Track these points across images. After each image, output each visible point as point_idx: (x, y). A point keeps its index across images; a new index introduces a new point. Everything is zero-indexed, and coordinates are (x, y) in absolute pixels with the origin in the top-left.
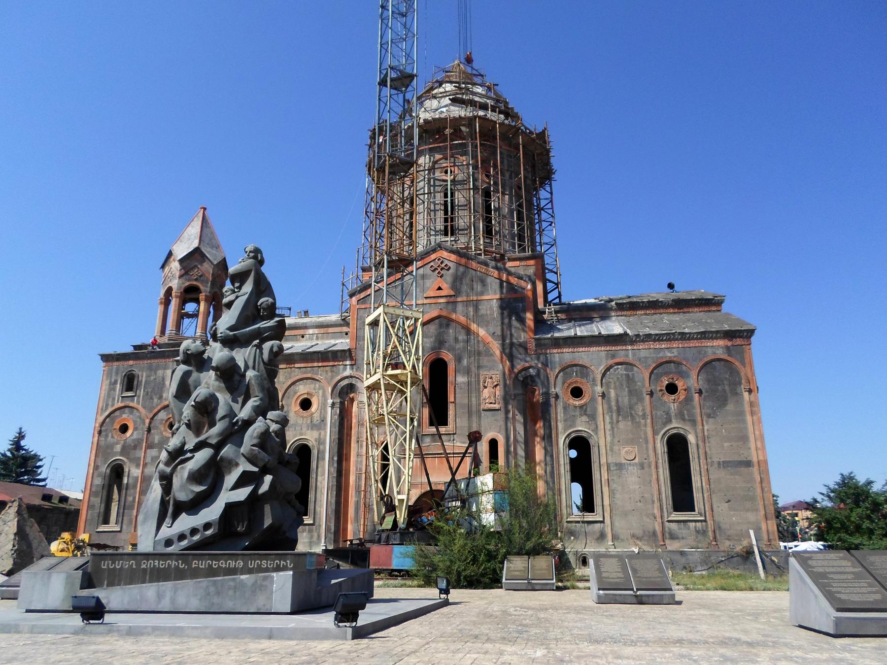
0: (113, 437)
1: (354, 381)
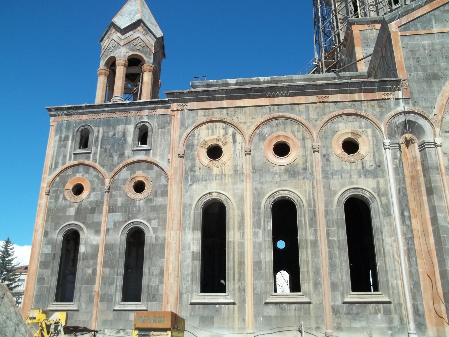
0: (64, 198)
1: (412, 117)
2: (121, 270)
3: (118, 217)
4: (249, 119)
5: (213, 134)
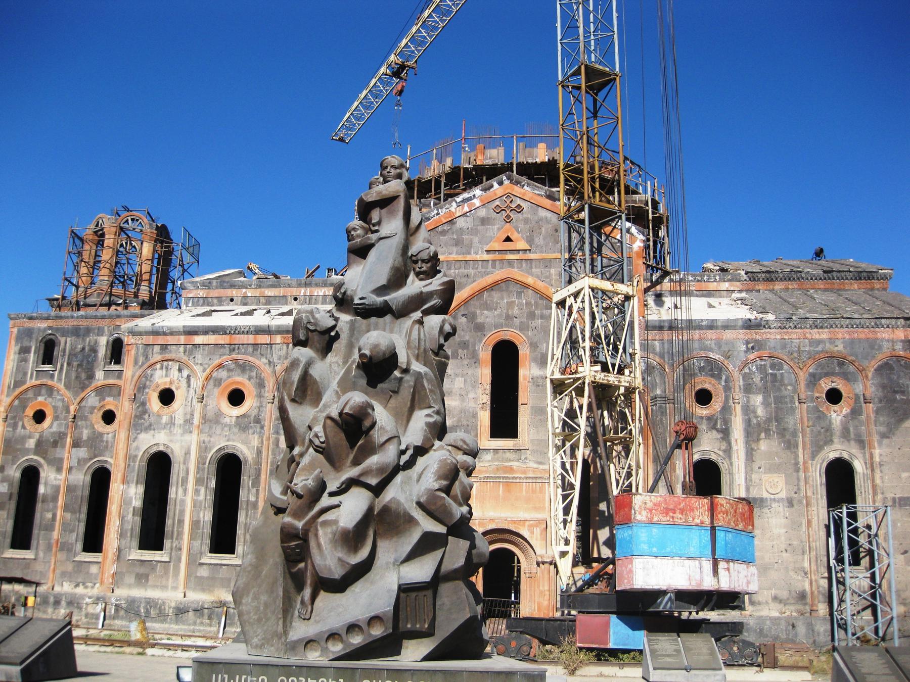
0: (24, 427)
2: (84, 516)
3: (82, 452)
4: (207, 361)
5: (167, 376)
